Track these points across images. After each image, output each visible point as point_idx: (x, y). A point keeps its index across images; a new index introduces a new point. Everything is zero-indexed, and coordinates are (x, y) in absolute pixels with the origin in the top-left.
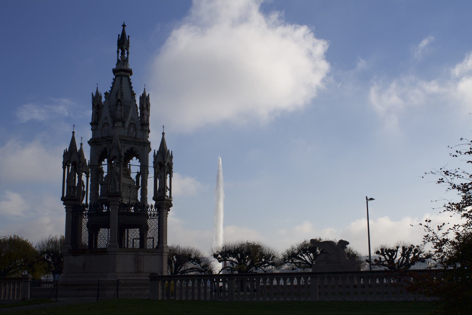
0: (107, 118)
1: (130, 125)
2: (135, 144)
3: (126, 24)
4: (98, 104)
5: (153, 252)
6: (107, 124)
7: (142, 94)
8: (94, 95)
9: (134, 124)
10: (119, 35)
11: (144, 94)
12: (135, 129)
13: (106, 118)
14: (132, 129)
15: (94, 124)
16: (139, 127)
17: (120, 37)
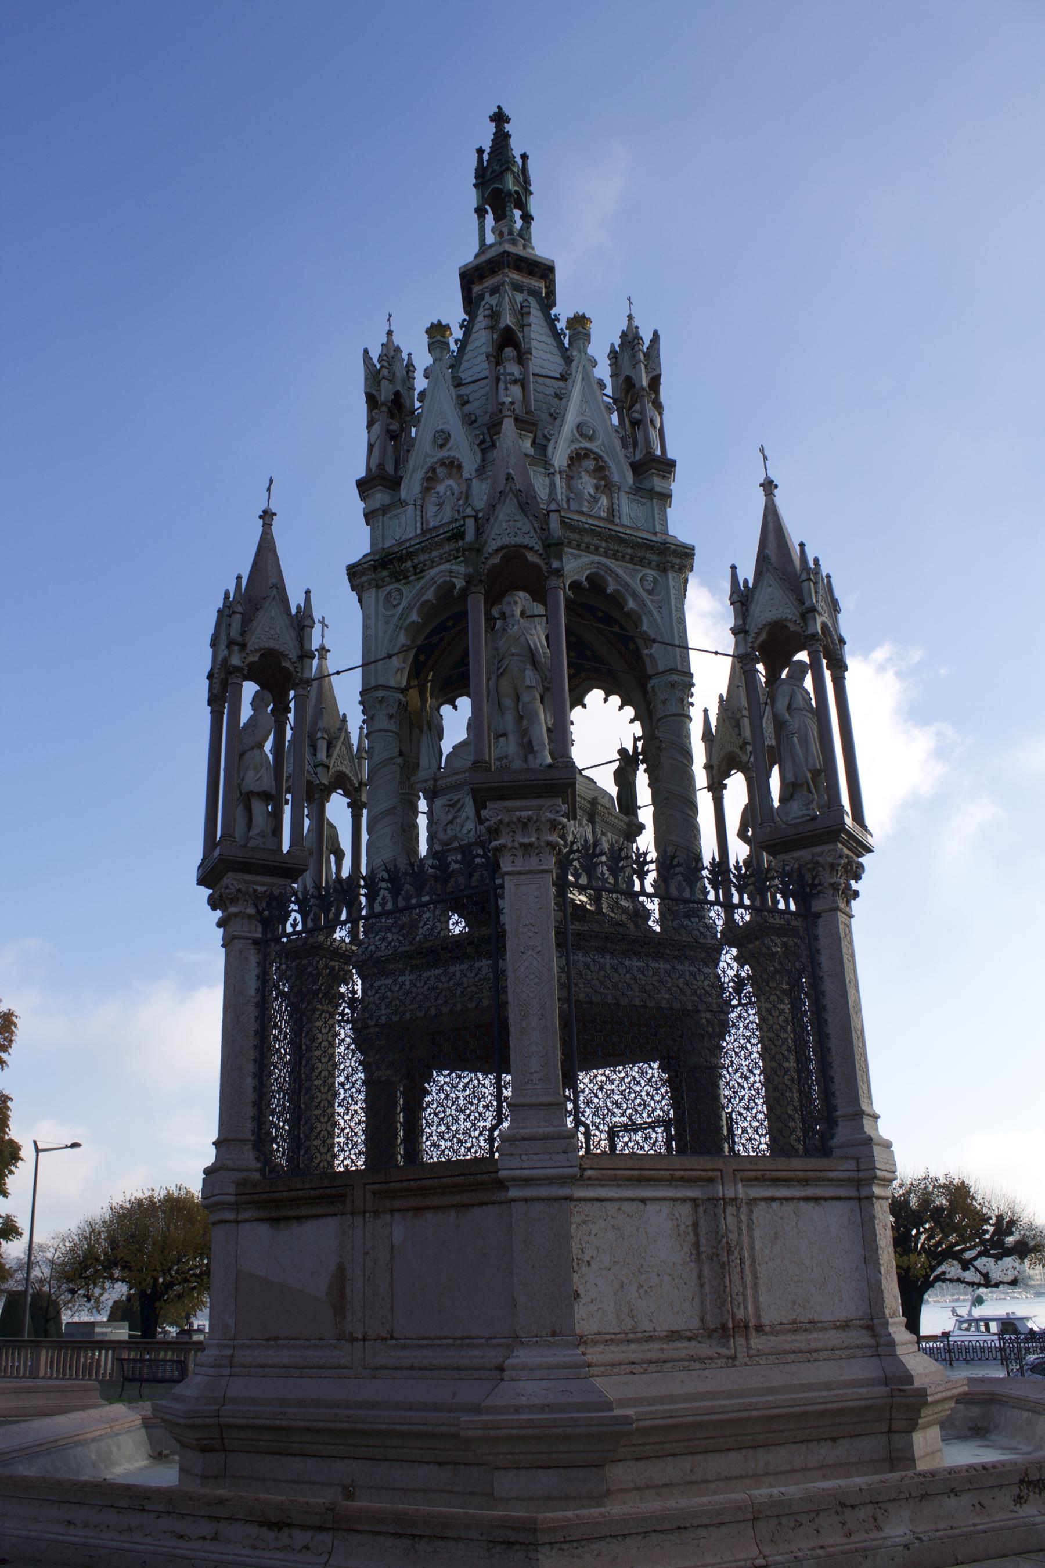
0: (447, 437)
1: (576, 458)
2: (615, 557)
3: (507, 111)
4: (397, 394)
5: (806, 1182)
6: (453, 466)
7: (624, 335)
8: (375, 355)
9: (598, 458)
10: (480, 151)
11: (630, 338)
12: (606, 486)
13: (443, 439)
14: (587, 484)
15: (379, 484)
16: (623, 475)
17: (486, 157)
